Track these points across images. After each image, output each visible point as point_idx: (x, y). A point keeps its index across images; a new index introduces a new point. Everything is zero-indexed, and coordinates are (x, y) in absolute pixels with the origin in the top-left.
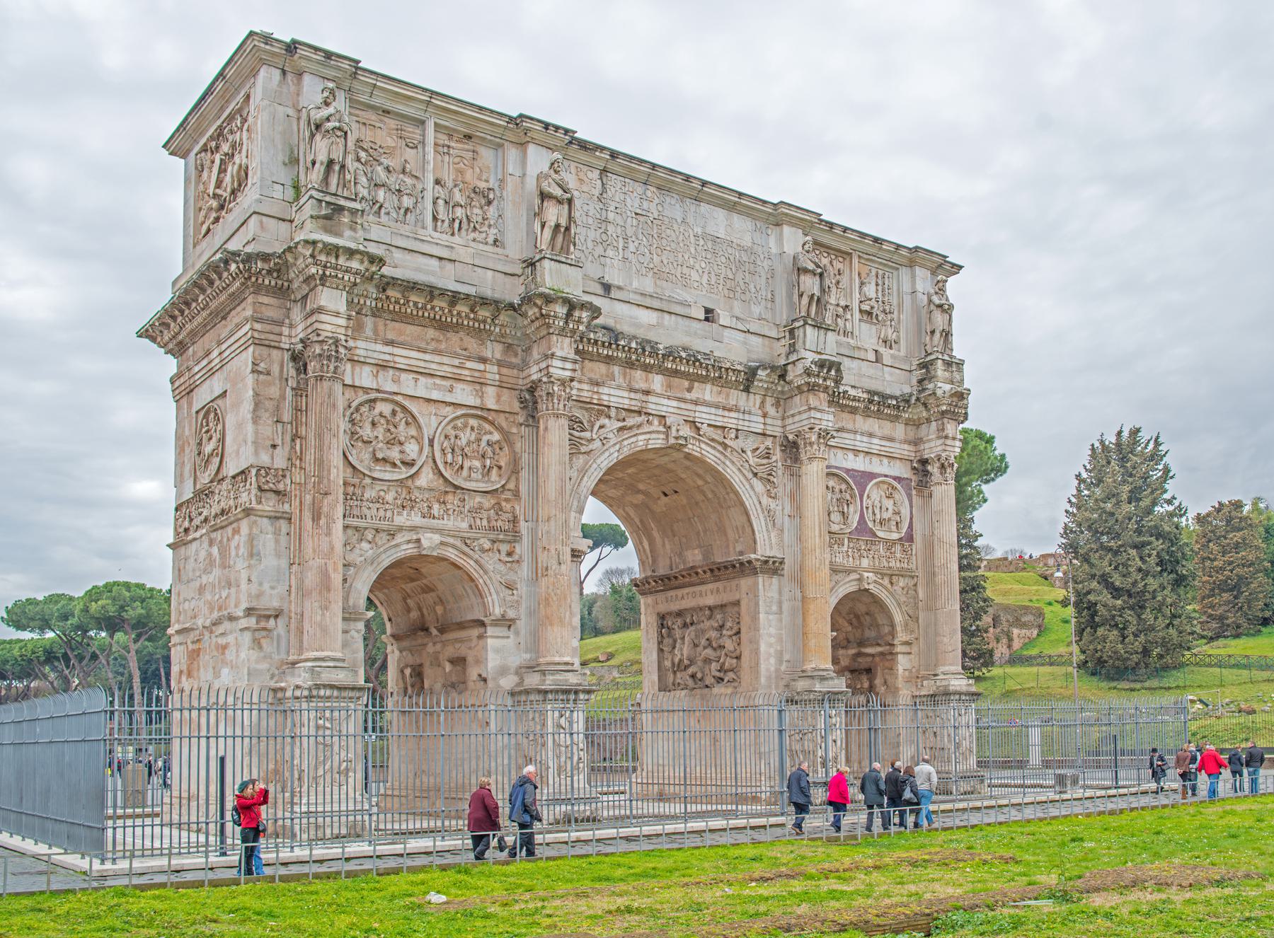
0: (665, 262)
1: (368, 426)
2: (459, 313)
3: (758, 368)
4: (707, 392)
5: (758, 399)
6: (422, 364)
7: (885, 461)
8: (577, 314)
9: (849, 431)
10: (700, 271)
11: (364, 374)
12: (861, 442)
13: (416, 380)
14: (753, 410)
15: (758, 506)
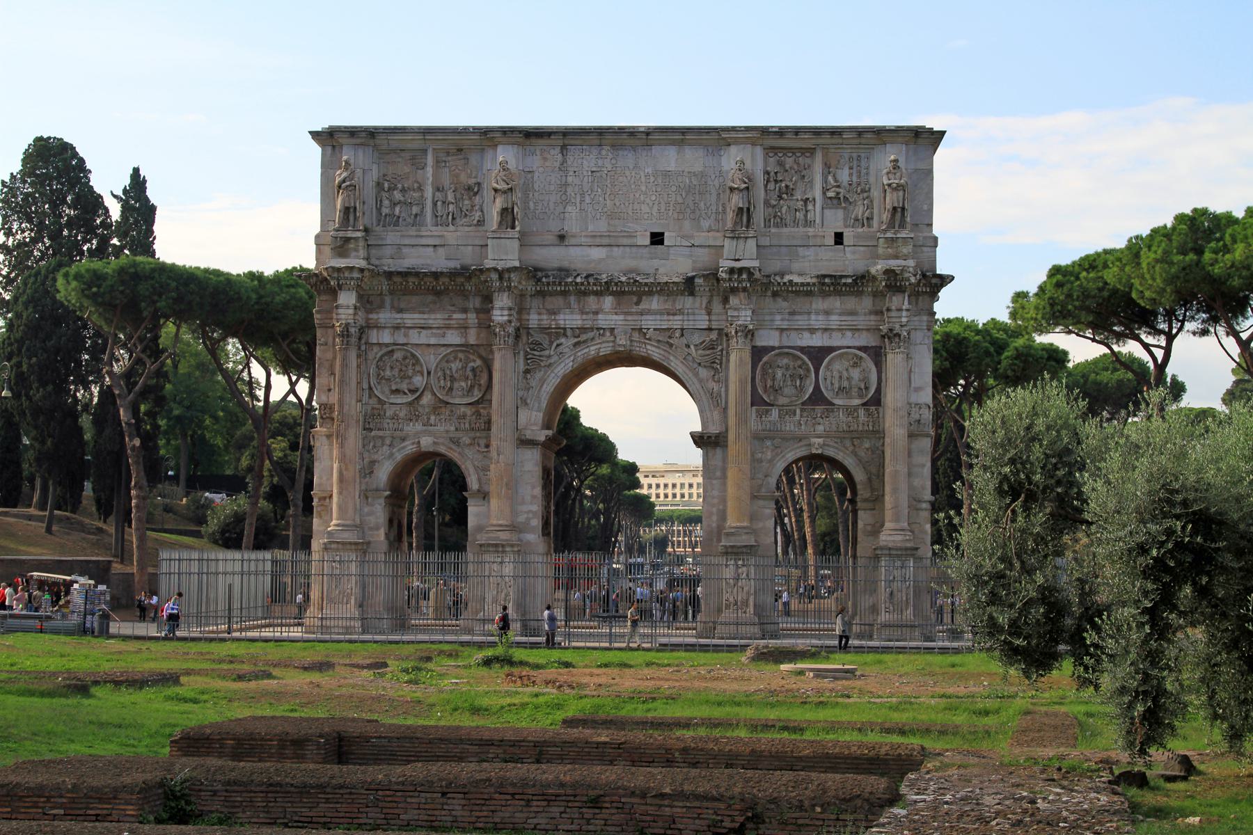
0: (618, 204)
1: (388, 368)
2: (444, 284)
3: (693, 278)
4: (655, 303)
5: (705, 301)
6: (423, 322)
7: (849, 334)
8: (506, 276)
9: (800, 314)
10: (651, 204)
11: (385, 335)
12: (817, 321)
13: (420, 333)
14: (697, 311)
15: (701, 391)
